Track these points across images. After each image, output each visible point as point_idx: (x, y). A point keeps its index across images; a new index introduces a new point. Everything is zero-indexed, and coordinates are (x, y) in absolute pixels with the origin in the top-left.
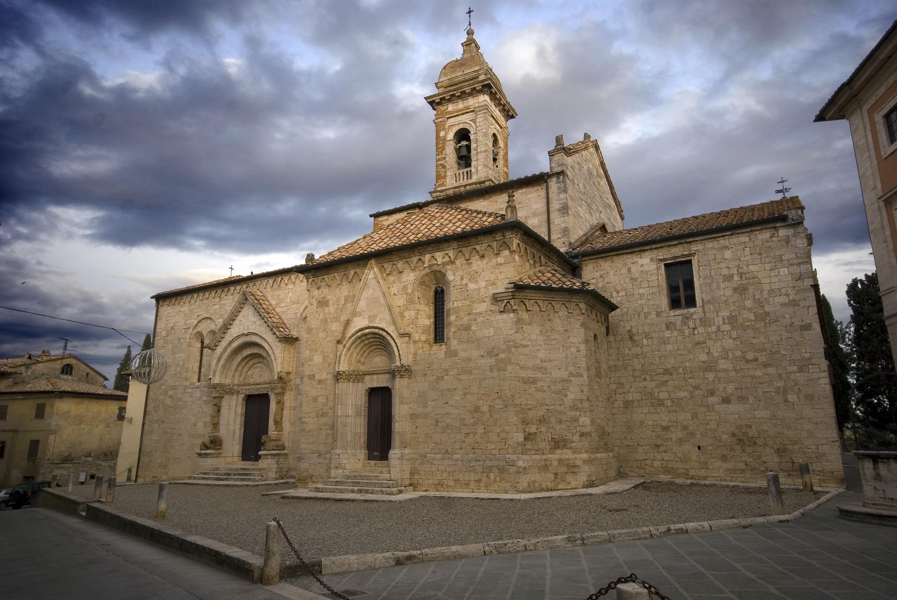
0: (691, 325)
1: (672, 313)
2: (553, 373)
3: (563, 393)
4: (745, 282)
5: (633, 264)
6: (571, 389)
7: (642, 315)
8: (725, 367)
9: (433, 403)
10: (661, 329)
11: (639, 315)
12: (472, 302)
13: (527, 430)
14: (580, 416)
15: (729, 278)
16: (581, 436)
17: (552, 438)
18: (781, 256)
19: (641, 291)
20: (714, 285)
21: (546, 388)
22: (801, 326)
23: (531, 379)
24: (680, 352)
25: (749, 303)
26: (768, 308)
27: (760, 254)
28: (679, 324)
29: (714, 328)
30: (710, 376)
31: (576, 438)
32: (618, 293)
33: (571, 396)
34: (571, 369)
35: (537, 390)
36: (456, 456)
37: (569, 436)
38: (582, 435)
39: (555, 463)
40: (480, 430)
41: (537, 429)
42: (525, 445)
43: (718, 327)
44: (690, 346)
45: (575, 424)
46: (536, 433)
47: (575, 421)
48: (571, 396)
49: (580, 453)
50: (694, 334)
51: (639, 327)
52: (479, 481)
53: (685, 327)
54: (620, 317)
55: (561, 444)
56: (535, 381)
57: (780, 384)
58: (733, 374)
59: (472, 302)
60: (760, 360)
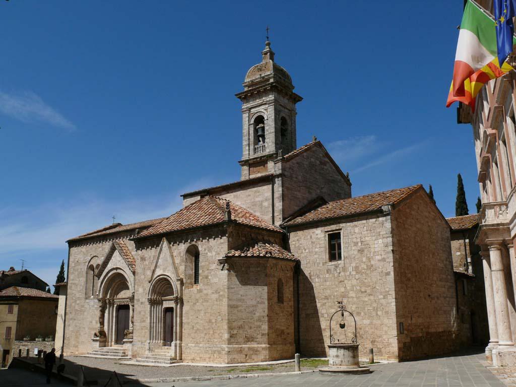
0: (338, 271)
3: (253, 313)
4: (363, 247)
8: (352, 295)
9: (191, 317)
12: (209, 263)
14: (262, 324)
15: (356, 244)
16: (262, 335)
17: (246, 337)
18: (379, 232)
21: (243, 310)
22: (386, 273)
25: (364, 259)
26: (373, 262)
27: (371, 230)
29: (348, 273)
31: (259, 336)
33: (257, 314)
34: (258, 300)
36: (201, 345)
39: (246, 349)
40: (211, 332)
43: (350, 273)
48: (257, 314)
49: (261, 344)
52: (210, 358)
55: (251, 339)
56: (237, 307)
57: (375, 305)
58: (355, 299)
59: (209, 263)
60: (367, 292)
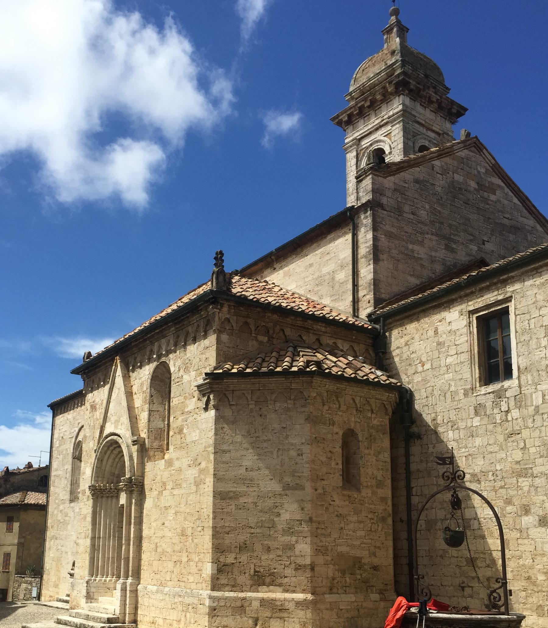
0: (504, 408)
1: (484, 390)
2: (262, 484)
5: (440, 321)
6: (286, 506)
7: (448, 395)
10: (469, 415)
11: (445, 396)
13: (221, 560)
16: (296, 569)
17: (255, 571)
19: (449, 360)
20: (533, 342)
23: (232, 494)
24: (490, 449)
28: (489, 404)
29: (531, 410)
30: (525, 483)
31: (289, 572)
32: (423, 366)
35: (238, 508)
37: (279, 569)
38: (298, 568)
41: (236, 558)
42: (218, 578)
44: (501, 438)
45: (289, 553)
46: (233, 564)
47: (290, 549)
48: (285, 516)
50: (507, 420)
51: (445, 413)
53: (496, 411)
54: (424, 401)
55: (268, 580)
